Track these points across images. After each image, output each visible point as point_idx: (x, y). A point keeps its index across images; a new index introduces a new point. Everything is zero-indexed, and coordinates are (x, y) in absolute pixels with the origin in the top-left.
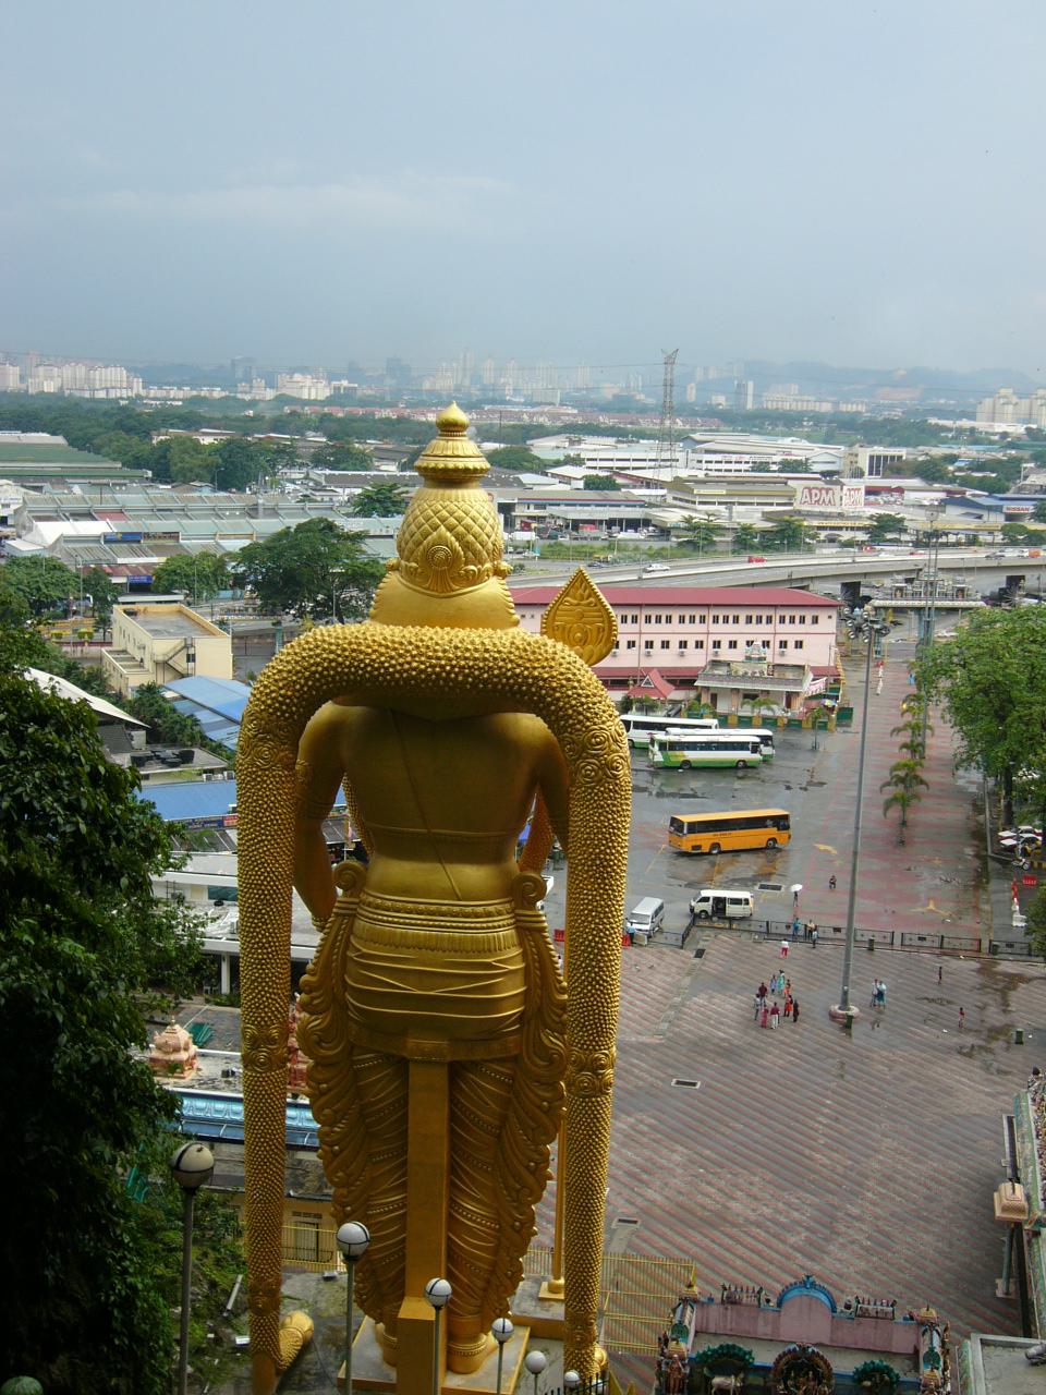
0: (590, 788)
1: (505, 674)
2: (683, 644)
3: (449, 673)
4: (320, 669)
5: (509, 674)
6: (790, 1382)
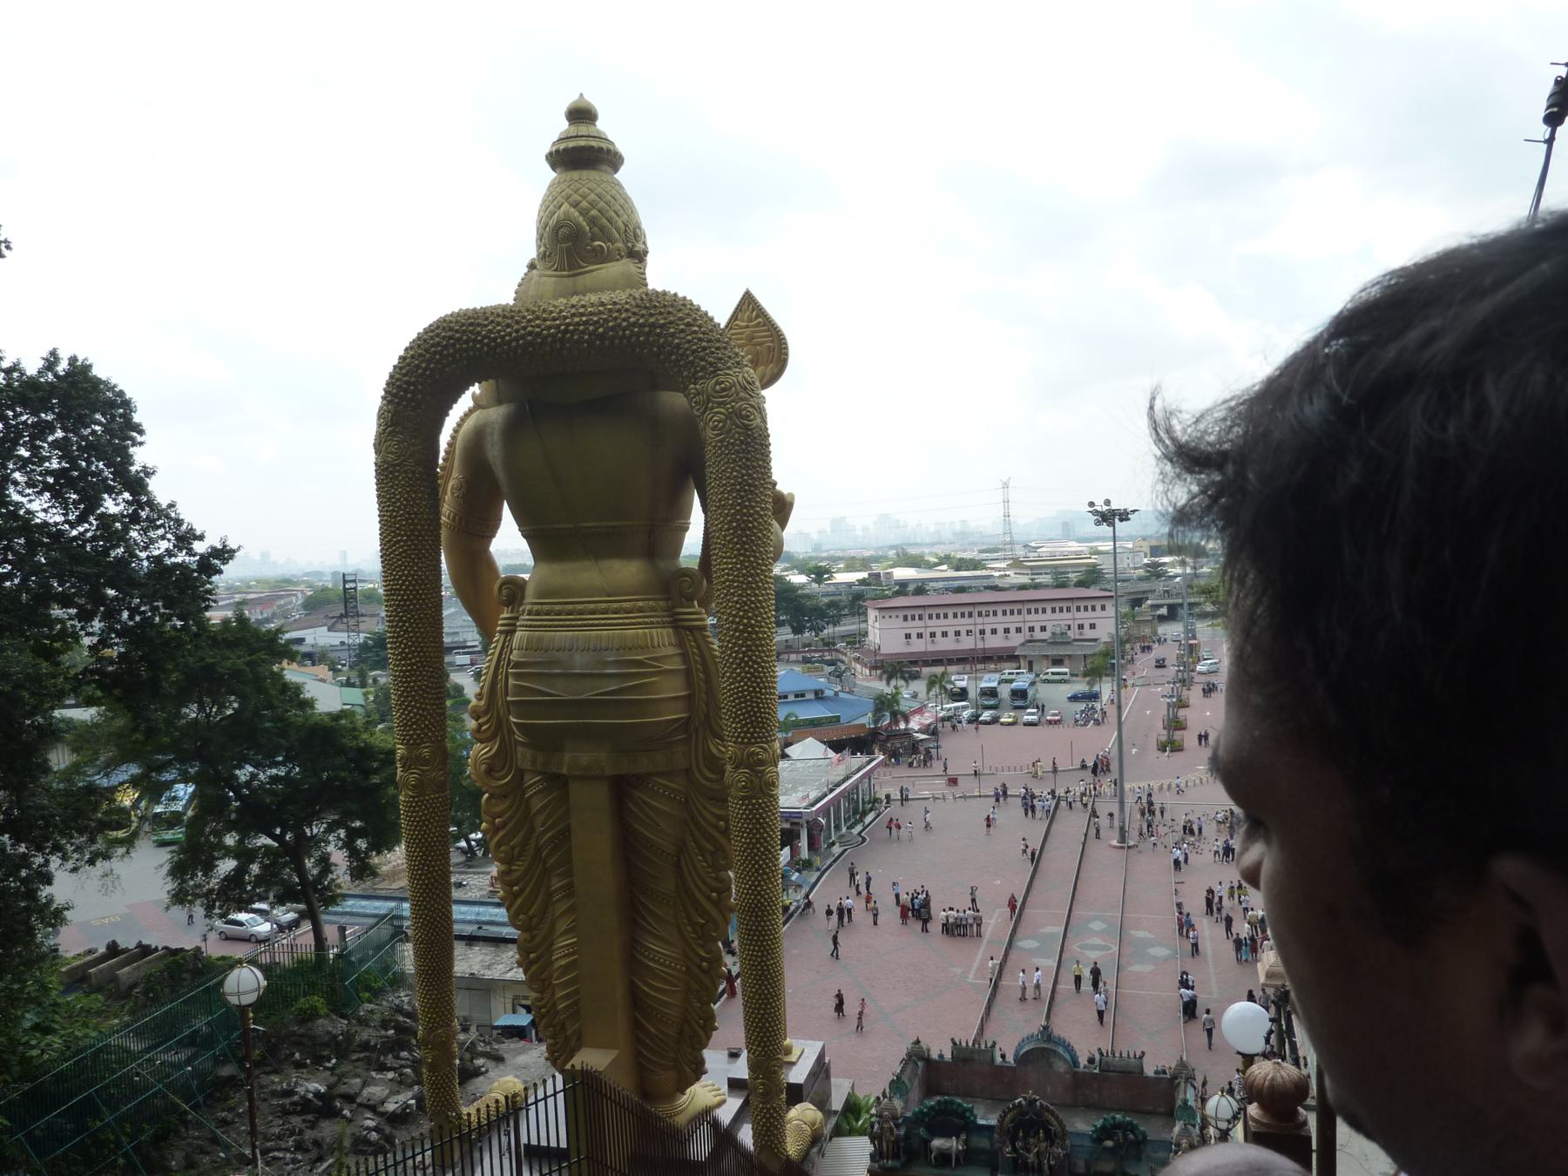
0: (718, 441)
1: (620, 325)
2: (1007, 631)
3: (566, 331)
4: (439, 348)
5: (625, 324)
6: (1019, 1144)
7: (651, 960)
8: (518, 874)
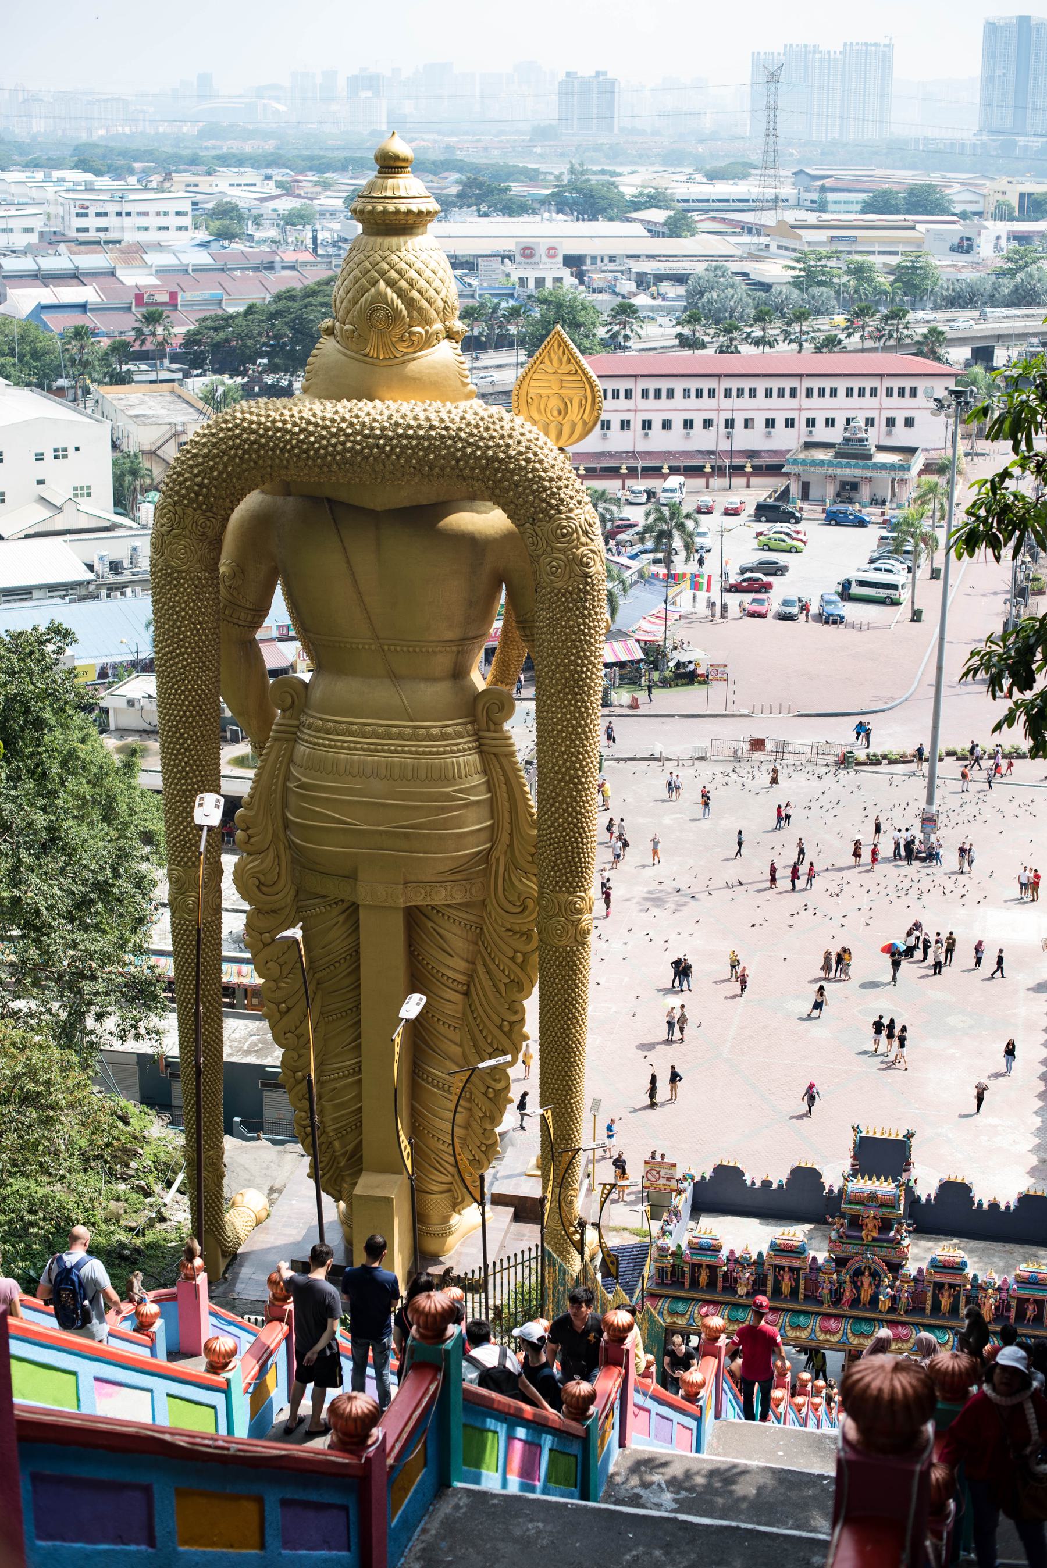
1: (454, 454)
2: (770, 423)
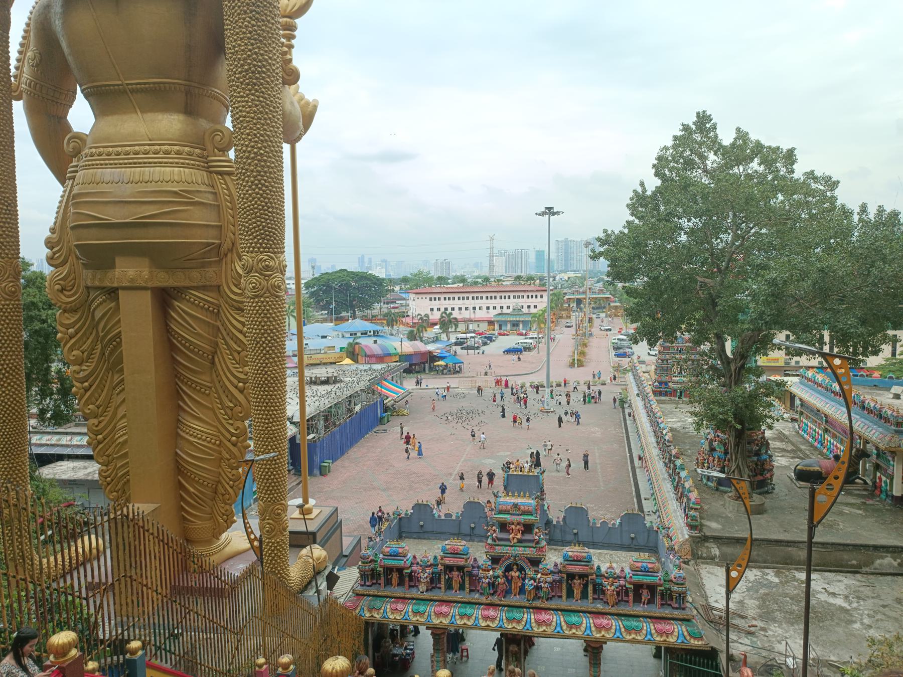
2: (488, 308)
7: (191, 435)
8: (87, 373)
